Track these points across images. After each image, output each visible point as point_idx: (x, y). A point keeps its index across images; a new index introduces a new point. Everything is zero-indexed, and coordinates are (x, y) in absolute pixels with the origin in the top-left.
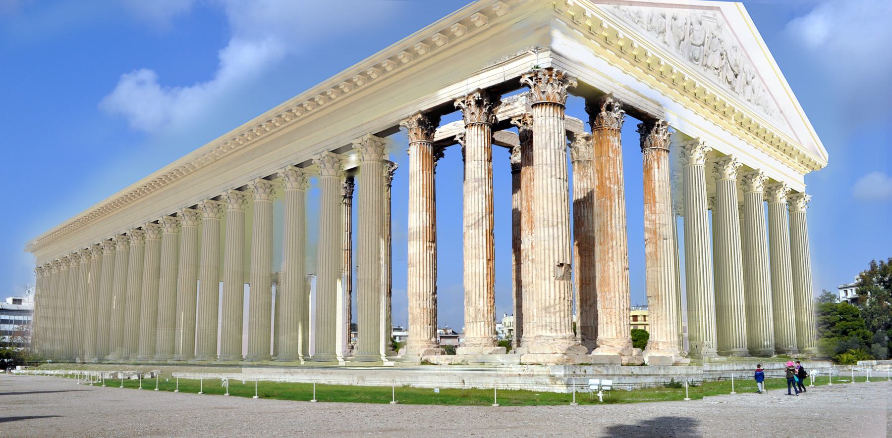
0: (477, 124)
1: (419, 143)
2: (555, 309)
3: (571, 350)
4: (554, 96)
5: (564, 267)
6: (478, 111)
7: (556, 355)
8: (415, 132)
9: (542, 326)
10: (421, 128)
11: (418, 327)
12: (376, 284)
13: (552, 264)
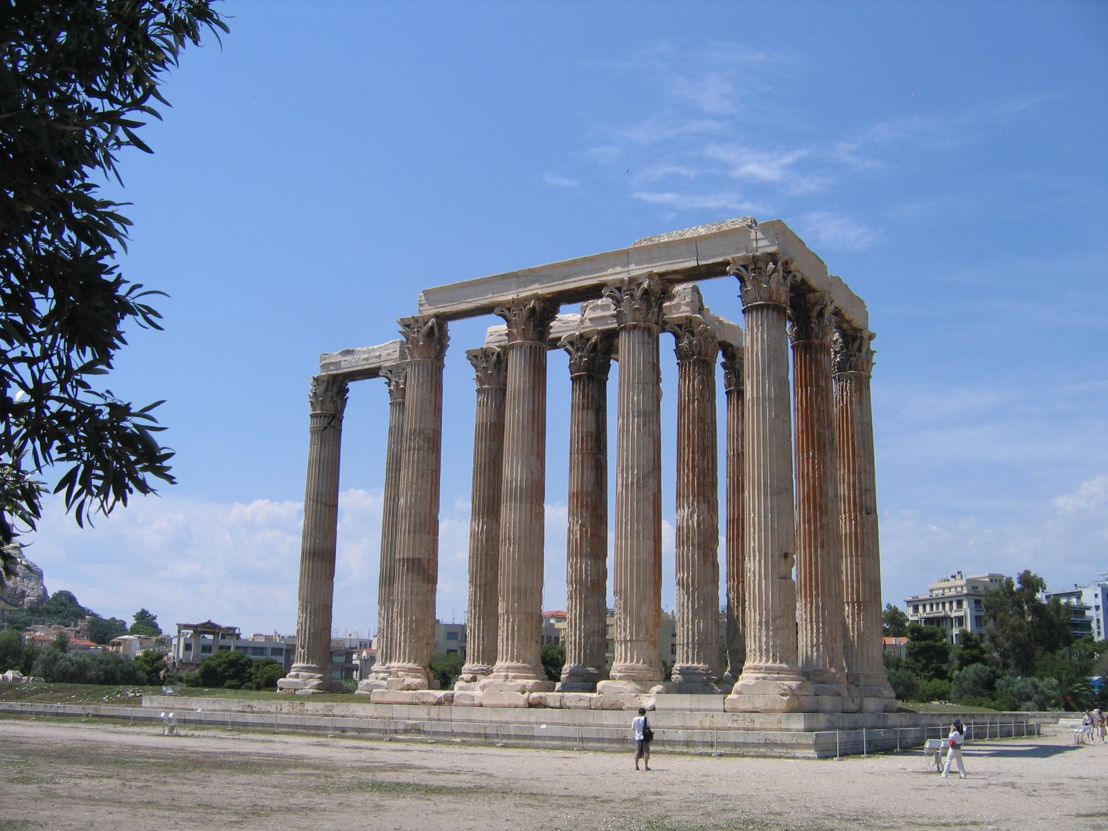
7: (785, 698)
12: (430, 567)
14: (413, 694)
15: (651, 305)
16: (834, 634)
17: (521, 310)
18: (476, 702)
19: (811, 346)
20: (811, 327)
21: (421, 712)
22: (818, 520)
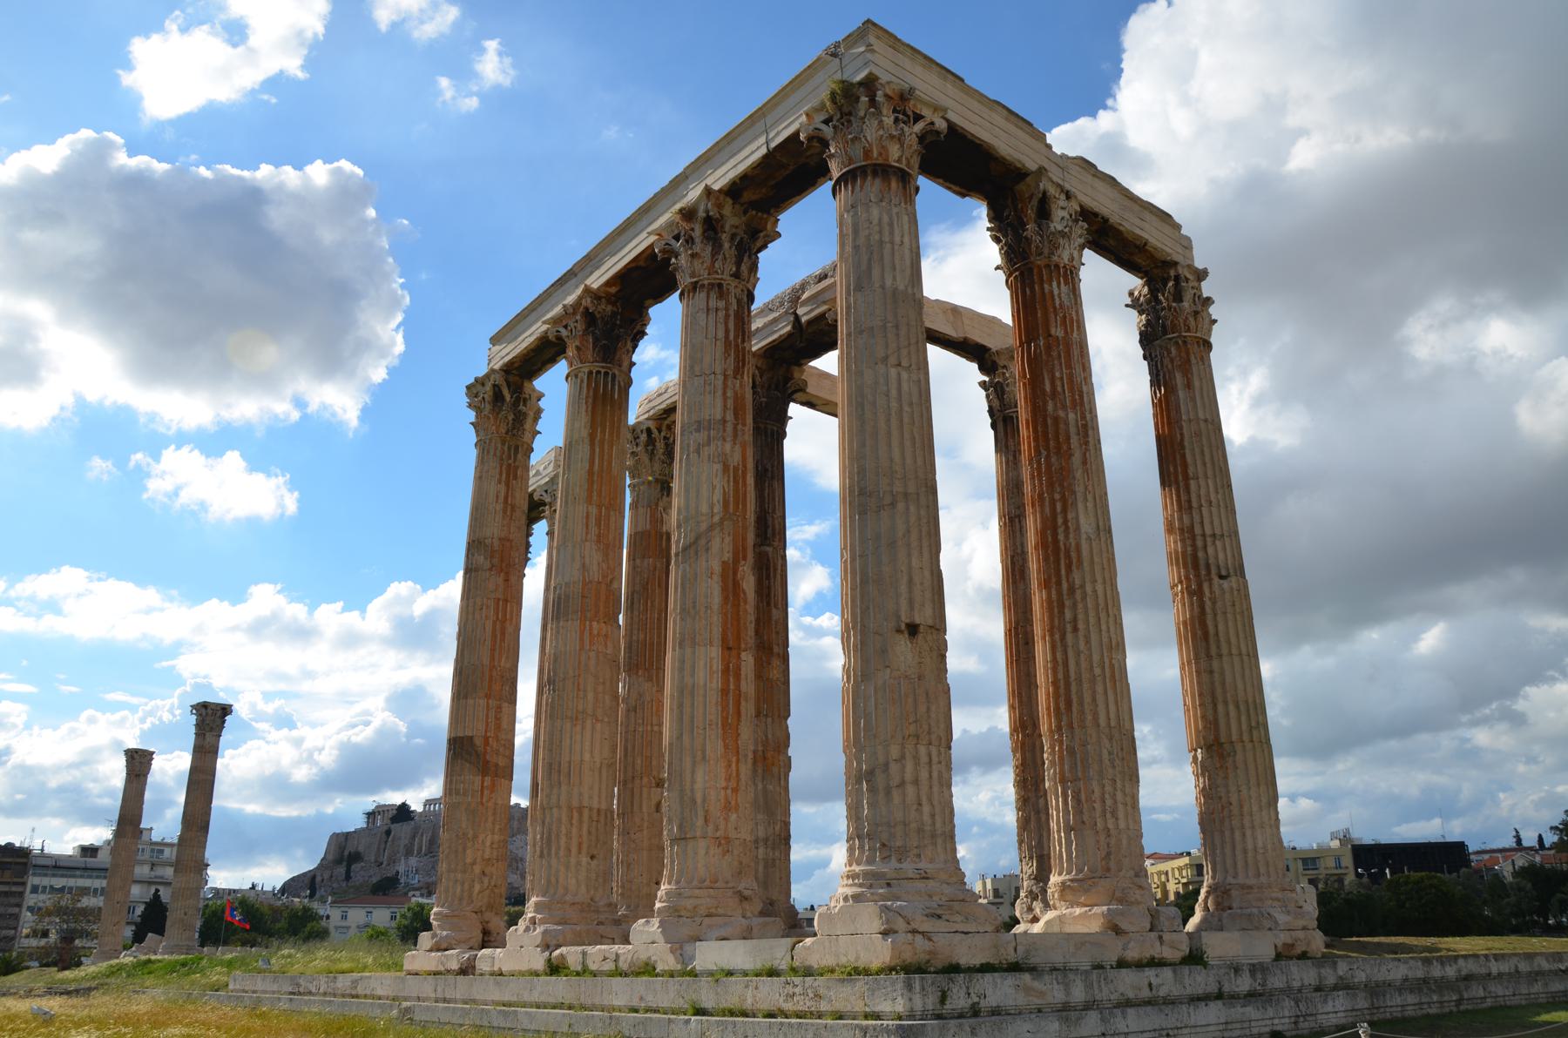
6: (710, 248)
10: (593, 333)
15: (721, 246)
18: (496, 969)
19: (1031, 270)
20: (1026, 238)
22: (1064, 578)
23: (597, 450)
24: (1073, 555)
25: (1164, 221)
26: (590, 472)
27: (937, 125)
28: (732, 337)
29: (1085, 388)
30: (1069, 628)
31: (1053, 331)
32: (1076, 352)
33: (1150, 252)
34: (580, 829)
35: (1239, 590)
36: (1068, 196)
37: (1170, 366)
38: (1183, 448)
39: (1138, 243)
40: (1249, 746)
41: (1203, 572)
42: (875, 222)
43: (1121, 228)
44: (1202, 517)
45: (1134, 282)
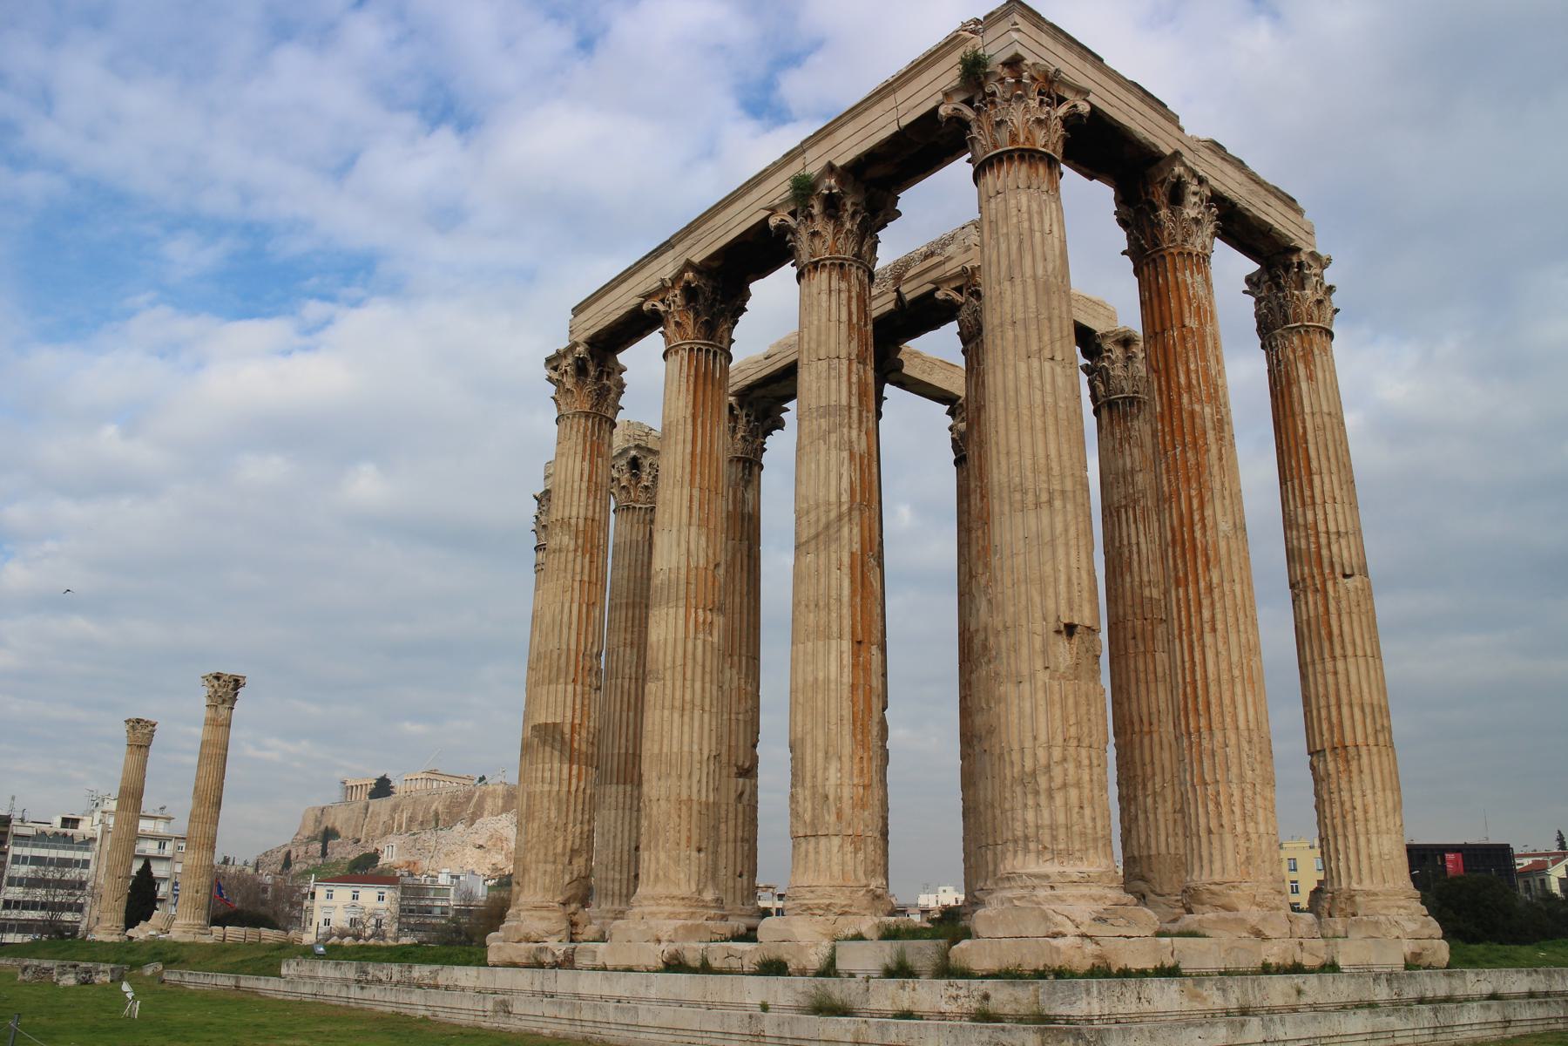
0: (828, 262)
1: (687, 347)
2: (1051, 779)
3: (1105, 921)
4: (1030, 132)
5: (1076, 638)
6: (830, 228)
7: (1059, 942)
8: (677, 319)
9: (1015, 841)
11: (662, 856)
12: (577, 737)
13: (1038, 627)
14: (530, 949)
15: (842, 225)
16: (1249, 806)
17: (676, 296)
18: (599, 962)
21: (523, 979)
23: (700, 431)
24: (1211, 553)
25: (1287, 205)
26: (693, 454)
27: (1080, 108)
28: (855, 320)
29: (1220, 382)
30: (1207, 628)
31: (1187, 322)
32: (1210, 344)
33: (1273, 237)
34: (690, 822)
35: (1363, 590)
36: (1201, 181)
37: (1291, 357)
38: (1306, 442)
39: (1263, 228)
40: (1374, 750)
41: (1327, 571)
42: (1024, 209)
43: (1248, 213)
44: (1325, 514)
45: (1252, 267)
